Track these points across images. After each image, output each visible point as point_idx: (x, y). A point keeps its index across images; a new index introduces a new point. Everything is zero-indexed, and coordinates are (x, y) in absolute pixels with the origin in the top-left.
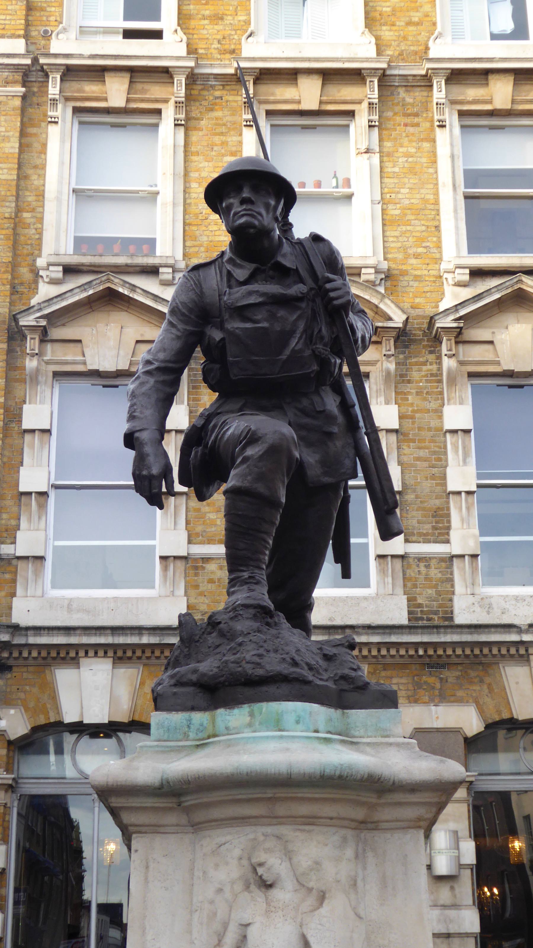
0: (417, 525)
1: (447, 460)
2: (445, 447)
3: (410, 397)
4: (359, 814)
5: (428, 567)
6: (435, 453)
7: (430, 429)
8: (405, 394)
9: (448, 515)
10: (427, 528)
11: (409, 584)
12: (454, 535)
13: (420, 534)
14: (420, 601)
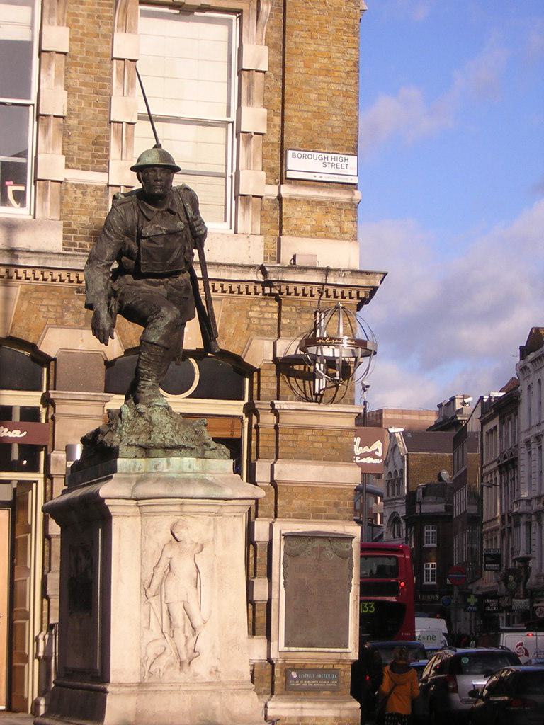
0: (77, 151)
1: (111, 88)
2: (111, 75)
3: (81, 19)
4: (216, 509)
5: (84, 194)
6: (101, 79)
7: (98, 54)
8: (76, 15)
9: (108, 145)
10: (86, 155)
11: (65, 210)
12: (114, 164)
13: (80, 161)
14: (74, 227)
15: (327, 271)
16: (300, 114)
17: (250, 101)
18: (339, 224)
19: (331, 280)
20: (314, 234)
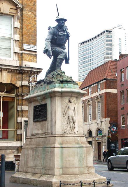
15: (32, 68)
16: (26, 37)
17: (16, 34)
18: (34, 59)
19: (33, 70)
20: (29, 61)
